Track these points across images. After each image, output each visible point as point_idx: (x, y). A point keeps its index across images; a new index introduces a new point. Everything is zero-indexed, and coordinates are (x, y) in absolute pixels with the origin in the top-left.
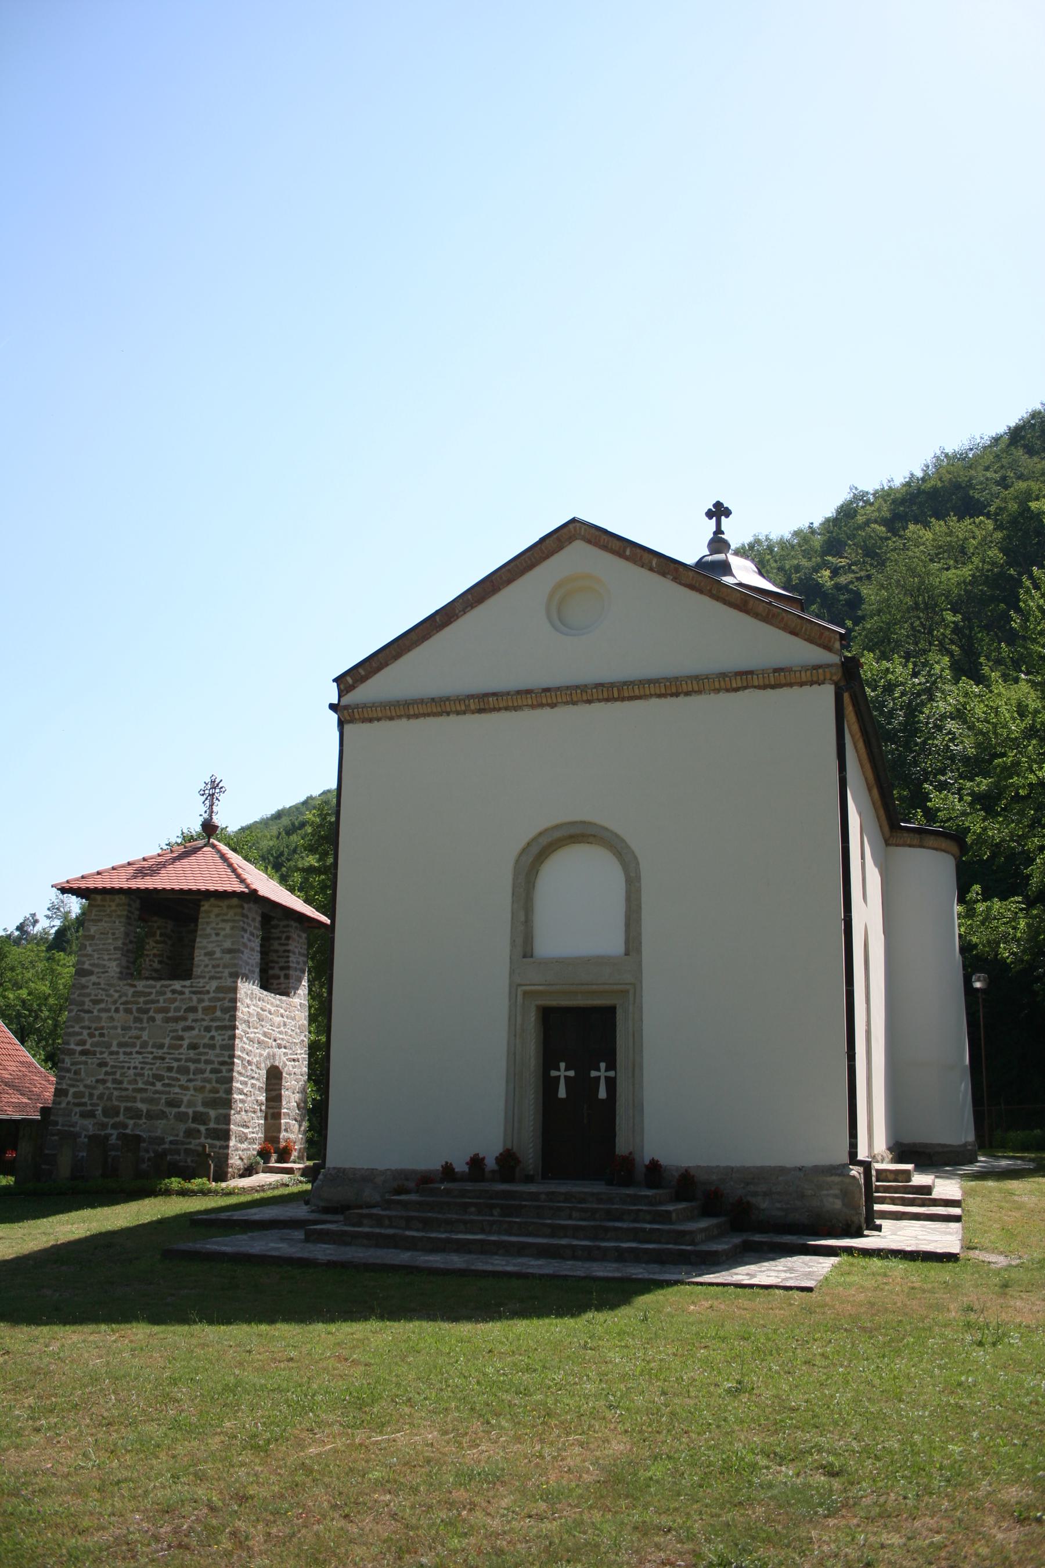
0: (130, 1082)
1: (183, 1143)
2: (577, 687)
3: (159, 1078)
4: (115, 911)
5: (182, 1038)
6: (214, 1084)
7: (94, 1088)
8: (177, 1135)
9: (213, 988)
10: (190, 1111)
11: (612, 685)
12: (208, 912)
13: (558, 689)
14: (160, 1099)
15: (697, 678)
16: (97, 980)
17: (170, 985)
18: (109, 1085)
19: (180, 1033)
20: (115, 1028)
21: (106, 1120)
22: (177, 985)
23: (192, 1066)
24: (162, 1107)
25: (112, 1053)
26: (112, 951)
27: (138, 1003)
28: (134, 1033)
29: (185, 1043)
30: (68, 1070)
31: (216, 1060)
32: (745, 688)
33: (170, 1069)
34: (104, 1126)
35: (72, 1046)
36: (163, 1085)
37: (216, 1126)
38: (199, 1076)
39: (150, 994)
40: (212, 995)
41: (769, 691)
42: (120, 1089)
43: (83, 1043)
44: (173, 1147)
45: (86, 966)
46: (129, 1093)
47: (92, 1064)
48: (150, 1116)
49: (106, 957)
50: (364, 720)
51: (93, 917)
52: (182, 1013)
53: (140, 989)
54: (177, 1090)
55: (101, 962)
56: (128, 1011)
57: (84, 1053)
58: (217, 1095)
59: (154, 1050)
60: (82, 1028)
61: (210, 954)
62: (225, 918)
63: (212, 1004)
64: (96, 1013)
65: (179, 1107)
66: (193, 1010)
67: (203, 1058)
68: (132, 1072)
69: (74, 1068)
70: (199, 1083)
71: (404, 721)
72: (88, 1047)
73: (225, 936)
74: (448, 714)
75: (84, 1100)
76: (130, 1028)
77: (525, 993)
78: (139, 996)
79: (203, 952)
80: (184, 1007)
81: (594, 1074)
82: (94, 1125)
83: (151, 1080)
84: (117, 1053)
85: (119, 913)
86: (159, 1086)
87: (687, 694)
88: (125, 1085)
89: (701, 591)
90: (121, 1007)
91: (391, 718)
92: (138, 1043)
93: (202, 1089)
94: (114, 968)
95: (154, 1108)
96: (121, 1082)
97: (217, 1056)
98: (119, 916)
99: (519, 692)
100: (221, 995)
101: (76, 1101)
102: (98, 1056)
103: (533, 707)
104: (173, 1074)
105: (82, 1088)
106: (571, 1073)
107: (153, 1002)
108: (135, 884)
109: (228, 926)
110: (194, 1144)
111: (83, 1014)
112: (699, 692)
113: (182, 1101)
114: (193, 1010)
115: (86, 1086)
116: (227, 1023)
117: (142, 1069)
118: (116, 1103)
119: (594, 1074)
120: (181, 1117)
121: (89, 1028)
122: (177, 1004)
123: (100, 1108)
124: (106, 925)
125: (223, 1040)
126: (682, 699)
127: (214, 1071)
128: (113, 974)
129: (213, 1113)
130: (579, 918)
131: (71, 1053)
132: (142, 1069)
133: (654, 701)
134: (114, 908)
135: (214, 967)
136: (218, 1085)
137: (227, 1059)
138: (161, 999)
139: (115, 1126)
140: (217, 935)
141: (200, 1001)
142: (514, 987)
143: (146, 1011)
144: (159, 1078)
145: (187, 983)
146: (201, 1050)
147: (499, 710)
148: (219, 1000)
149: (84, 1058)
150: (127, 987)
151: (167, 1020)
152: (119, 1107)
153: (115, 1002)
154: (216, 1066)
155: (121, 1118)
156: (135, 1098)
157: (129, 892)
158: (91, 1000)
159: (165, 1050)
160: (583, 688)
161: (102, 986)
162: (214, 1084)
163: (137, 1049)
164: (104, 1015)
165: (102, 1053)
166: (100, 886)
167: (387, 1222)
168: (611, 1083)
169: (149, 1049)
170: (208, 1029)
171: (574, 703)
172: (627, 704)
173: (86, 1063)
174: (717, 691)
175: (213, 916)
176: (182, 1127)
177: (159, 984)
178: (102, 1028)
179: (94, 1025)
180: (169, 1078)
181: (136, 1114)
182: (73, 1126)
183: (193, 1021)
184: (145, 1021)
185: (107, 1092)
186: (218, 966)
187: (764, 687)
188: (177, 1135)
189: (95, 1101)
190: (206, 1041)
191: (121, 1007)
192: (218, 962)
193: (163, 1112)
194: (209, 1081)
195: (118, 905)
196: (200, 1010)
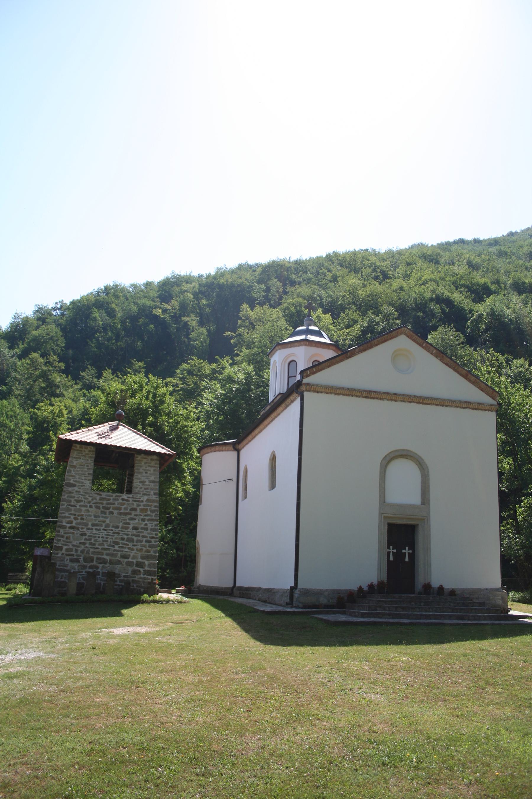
0: (100, 545)
1: (131, 577)
2: (408, 395)
3: (117, 543)
4: (88, 454)
5: (129, 524)
6: (148, 548)
7: (78, 547)
8: (127, 573)
9: (145, 500)
10: (134, 561)
11: (420, 397)
12: (140, 461)
14: (117, 554)
15: (451, 401)
16: (78, 490)
17: (121, 496)
18: (87, 545)
19: (128, 521)
20: (90, 516)
21: (85, 564)
22: (125, 496)
23: (135, 539)
25: (88, 529)
26: (87, 475)
27: (102, 504)
28: (101, 519)
29: (131, 526)
30: (63, 537)
31: (148, 536)
32: (466, 408)
33: (123, 539)
34: (84, 567)
35: (64, 524)
36: (119, 547)
37: (149, 569)
38: (139, 544)
40: (145, 503)
41: (475, 411)
42: (94, 548)
43: (71, 522)
44: (125, 579)
45: (72, 482)
46: (100, 550)
47: (77, 534)
48: (111, 562)
49: (83, 478)
50: (314, 391)
51: (75, 456)
52: (128, 511)
53: (103, 496)
54: (127, 550)
55: (80, 480)
57: (71, 528)
58: (149, 554)
59: (113, 529)
60: (71, 514)
61: (143, 482)
62: (150, 465)
63: (145, 508)
64: (78, 507)
65: (128, 558)
66: (135, 510)
67: (141, 534)
68: (101, 539)
69: (66, 536)
70: (139, 547)
71: (333, 395)
72: (74, 524)
73: (150, 474)
74: (352, 396)
75: (72, 553)
76: (99, 517)
77: (384, 517)
78: (103, 500)
79: (139, 481)
80: (130, 508)
81: (404, 551)
82: (79, 566)
83: (112, 544)
84: (92, 529)
85: (90, 455)
86: (116, 547)
87: (446, 406)
88: (97, 546)
89: (450, 367)
90: (93, 505)
91: (327, 393)
93: (141, 550)
94: (88, 484)
95: (114, 558)
96: (94, 544)
97: (149, 534)
98: (91, 457)
99: (384, 393)
100: (150, 504)
101: (68, 553)
102: (80, 530)
103: (388, 400)
104: (124, 542)
105: (71, 547)
106: (395, 551)
107: (111, 504)
108: (99, 441)
109: (152, 469)
110: (137, 577)
111: (70, 507)
112: (451, 406)
113: (130, 556)
114: (135, 510)
115: (73, 545)
116: (154, 518)
117: (107, 538)
118: (92, 555)
119: (404, 551)
120: (130, 564)
121: (75, 515)
122: (125, 506)
123: (82, 557)
124: (83, 461)
125: (152, 526)
126: (444, 408)
127: (146, 541)
128: (87, 487)
129: (147, 563)
130: (404, 489)
131: (65, 527)
132: (107, 538)
133: (434, 406)
134: (87, 452)
135: (145, 489)
136: (150, 549)
137: (154, 536)
138: (116, 503)
139: (91, 567)
140: (146, 473)
141: (139, 505)
142: (380, 514)
143: (108, 508)
144: (117, 543)
145: (131, 496)
146: (140, 530)
147: (374, 398)
148: (149, 506)
149: (72, 531)
150: (96, 495)
151: (121, 514)
152: (93, 557)
153: (89, 502)
154: (149, 539)
155: (95, 563)
156: (103, 553)
158: (75, 500)
159: (120, 529)
160: (410, 396)
161: (81, 493)
162: (148, 548)
163: (103, 527)
164: (83, 509)
165: (82, 528)
166: (78, 439)
167: (387, 609)
168: (412, 556)
169: (110, 528)
170: (143, 520)
171: (404, 402)
173: (73, 533)
174: (457, 407)
175: (143, 463)
176: (130, 569)
177: (114, 495)
178: (82, 515)
179: (77, 514)
180: (122, 544)
181: (104, 562)
182: (65, 566)
183: (135, 515)
184: (108, 513)
185: (86, 549)
186: (148, 489)
187: (473, 409)
188: (127, 573)
189: (79, 553)
190: (143, 526)
191: (93, 505)
192: (147, 487)
193: (119, 561)
194: (145, 546)
195: (90, 451)
196: (138, 510)
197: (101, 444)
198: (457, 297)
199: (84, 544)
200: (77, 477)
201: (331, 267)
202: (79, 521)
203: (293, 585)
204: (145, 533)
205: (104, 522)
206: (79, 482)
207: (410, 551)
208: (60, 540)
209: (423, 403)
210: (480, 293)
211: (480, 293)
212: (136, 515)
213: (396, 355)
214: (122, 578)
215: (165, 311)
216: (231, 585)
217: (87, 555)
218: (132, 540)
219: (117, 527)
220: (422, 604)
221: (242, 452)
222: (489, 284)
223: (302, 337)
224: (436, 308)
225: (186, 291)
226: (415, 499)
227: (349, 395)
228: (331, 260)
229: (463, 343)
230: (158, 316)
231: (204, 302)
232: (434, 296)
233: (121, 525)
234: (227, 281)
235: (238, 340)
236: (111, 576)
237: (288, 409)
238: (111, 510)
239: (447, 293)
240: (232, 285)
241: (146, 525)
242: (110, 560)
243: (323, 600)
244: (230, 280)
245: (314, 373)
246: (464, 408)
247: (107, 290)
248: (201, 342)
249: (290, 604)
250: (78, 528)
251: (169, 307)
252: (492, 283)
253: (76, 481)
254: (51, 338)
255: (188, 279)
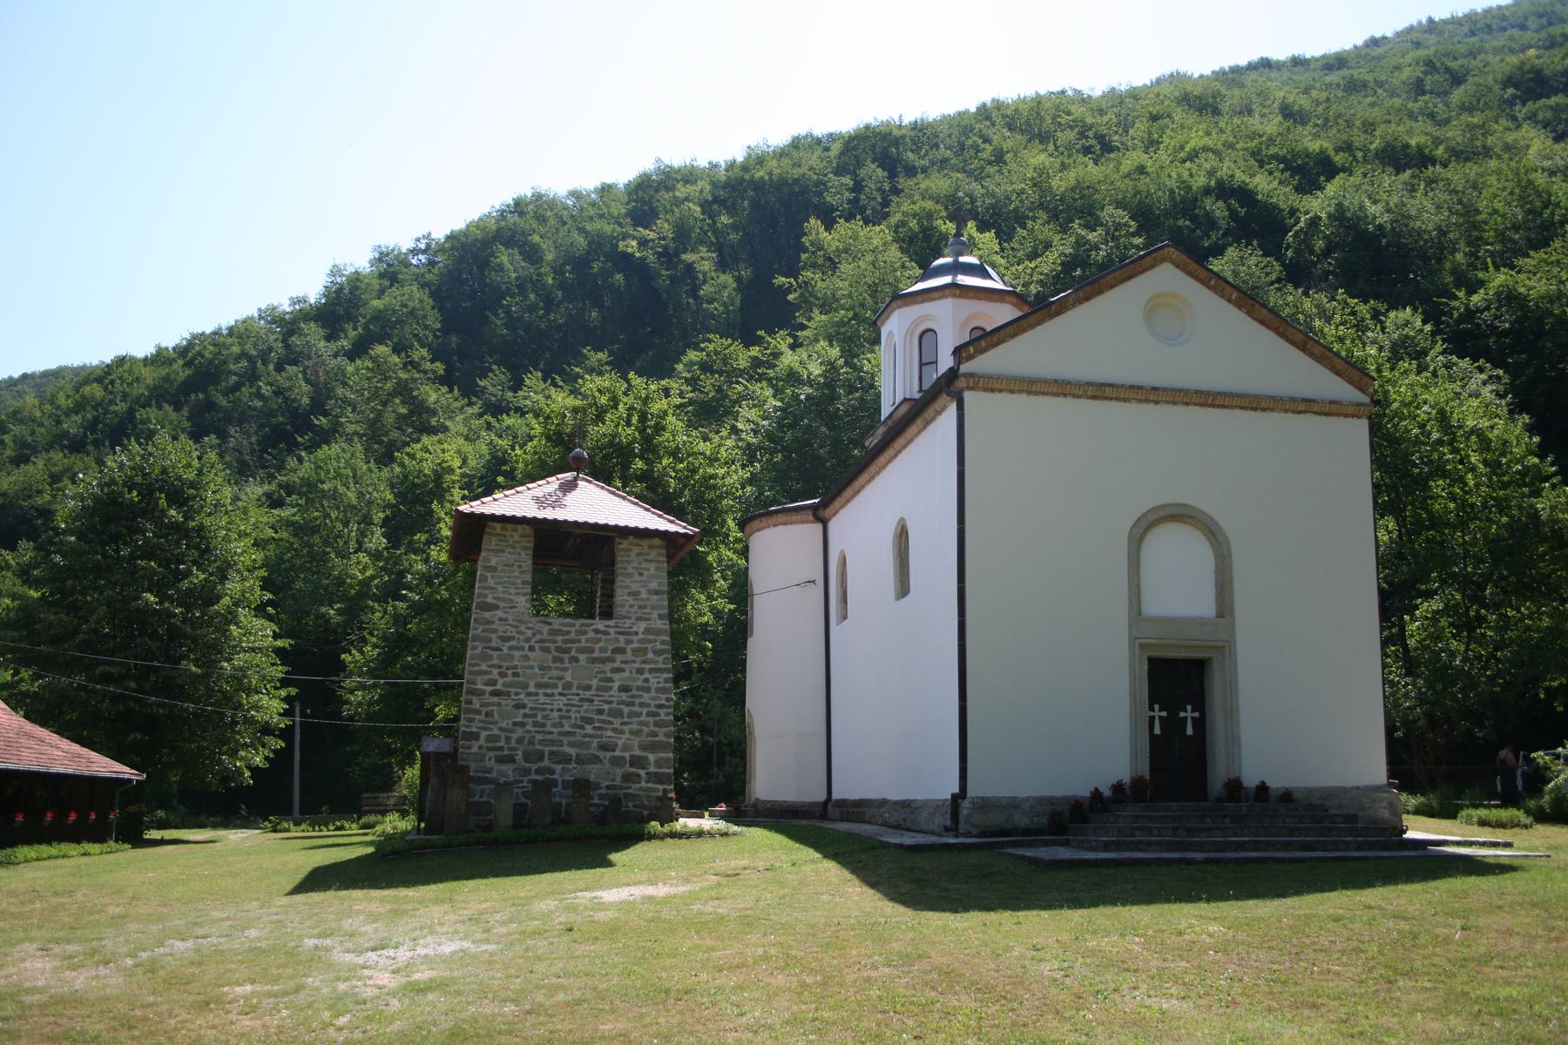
0: (554, 725)
1: (621, 788)
2: (1181, 390)
3: (589, 721)
5: (611, 680)
7: (511, 731)
10: (627, 755)
11: (1208, 393)
12: (627, 550)
13: (1165, 389)
15: (1274, 398)
18: (529, 727)
20: (532, 667)
22: (599, 624)
24: (594, 750)
25: (530, 694)
27: (555, 642)
28: (554, 673)
29: (616, 685)
30: (478, 712)
32: (1306, 412)
33: (600, 712)
34: (527, 772)
38: (635, 720)
39: (569, 633)
43: (494, 683)
45: (489, 600)
46: (555, 736)
48: (580, 760)
49: (513, 591)
50: (986, 389)
52: (609, 653)
53: (556, 627)
54: (610, 733)
56: (546, 650)
64: (506, 651)
66: (621, 651)
67: (637, 701)
68: (556, 714)
69: (484, 710)
70: (635, 727)
71: (1024, 395)
72: (499, 687)
74: (1065, 396)
76: (549, 668)
81: (1182, 714)
84: (537, 694)
86: (589, 729)
87: (1264, 410)
88: (549, 728)
91: (1012, 392)
92: (560, 684)
93: (638, 733)
94: (523, 603)
96: (544, 725)
99: (1131, 387)
103: (1140, 401)
104: (604, 717)
106: (1164, 714)
107: (573, 641)
108: (541, 514)
109: (652, 566)
110: (634, 788)
112: (1272, 410)
114: (621, 651)
115: (500, 729)
119: (1182, 714)
120: (618, 761)
126: (1258, 414)
127: (649, 714)
129: (652, 757)
130: (1179, 586)
131: (482, 693)
133: (1238, 411)
138: (583, 638)
139: (538, 772)
141: (628, 642)
142: (1132, 639)
143: (567, 651)
144: (589, 721)
145: (612, 623)
146: (634, 692)
148: (650, 641)
149: (496, 699)
151: (593, 661)
153: (528, 640)
155: (546, 763)
157: (533, 522)
160: (1185, 392)
164: (516, 654)
166: (499, 512)
168: (1200, 724)
170: (640, 671)
172: (1216, 411)
173: (499, 704)
174: (1286, 411)
176: (619, 771)
178: (515, 667)
179: (505, 664)
181: (566, 759)
187: (1320, 414)
189: (513, 744)
190: (639, 683)
194: (646, 724)
195: (522, 536)
196: (629, 652)
197: (545, 519)
198: (1262, 183)
199: (523, 725)
200: (500, 589)
201: (990, 132)
202: (509, 679)
203: (957, 790)
204: (646, 697)
205: (560, 678)
206: (504, 600)
207: (1196, 714)
208: (472, 720)
209: (1213, 406)
210: (1310, 173)
211: (1310, 173)
212: (626, 662)
213: (1154, 307)
214: (603, 791)
215: (643, 243)
216: (821, 796)
217: (530, 748)
218: (619, 714)
219: (588, 688)
220: (1227, 821)
221: (832, 525)
222: (1331, 153)
223: (947, 279)
224: (1219, 209)
225: (687, 199)
226: (1204, 606)
227: (1057, 395)
228: (988, 118)
229: (1278, 280)
230: (632, 255)
231: (725, 219)
232: (1213, 183)
233: (594, 683)
234: (770, 174)
235: (802, 295)
236: (582, 786)
237: (930, 428)
238: (573, 653)
239: (1240, 176)
240: (783, 182)
241: (646, 680)
242: (578, 755)
243: (1021, 820)
244: (777, 172)
245: (983, 351)
246: (1300, 412)
247: (519, 206)
248: (725, 305)
249: (953, 829)
250: (508, 694)
251: (652, 235)
252: (1337, 150)
253: (498, 599)
254: (412, 313)
255: (689, 175)
